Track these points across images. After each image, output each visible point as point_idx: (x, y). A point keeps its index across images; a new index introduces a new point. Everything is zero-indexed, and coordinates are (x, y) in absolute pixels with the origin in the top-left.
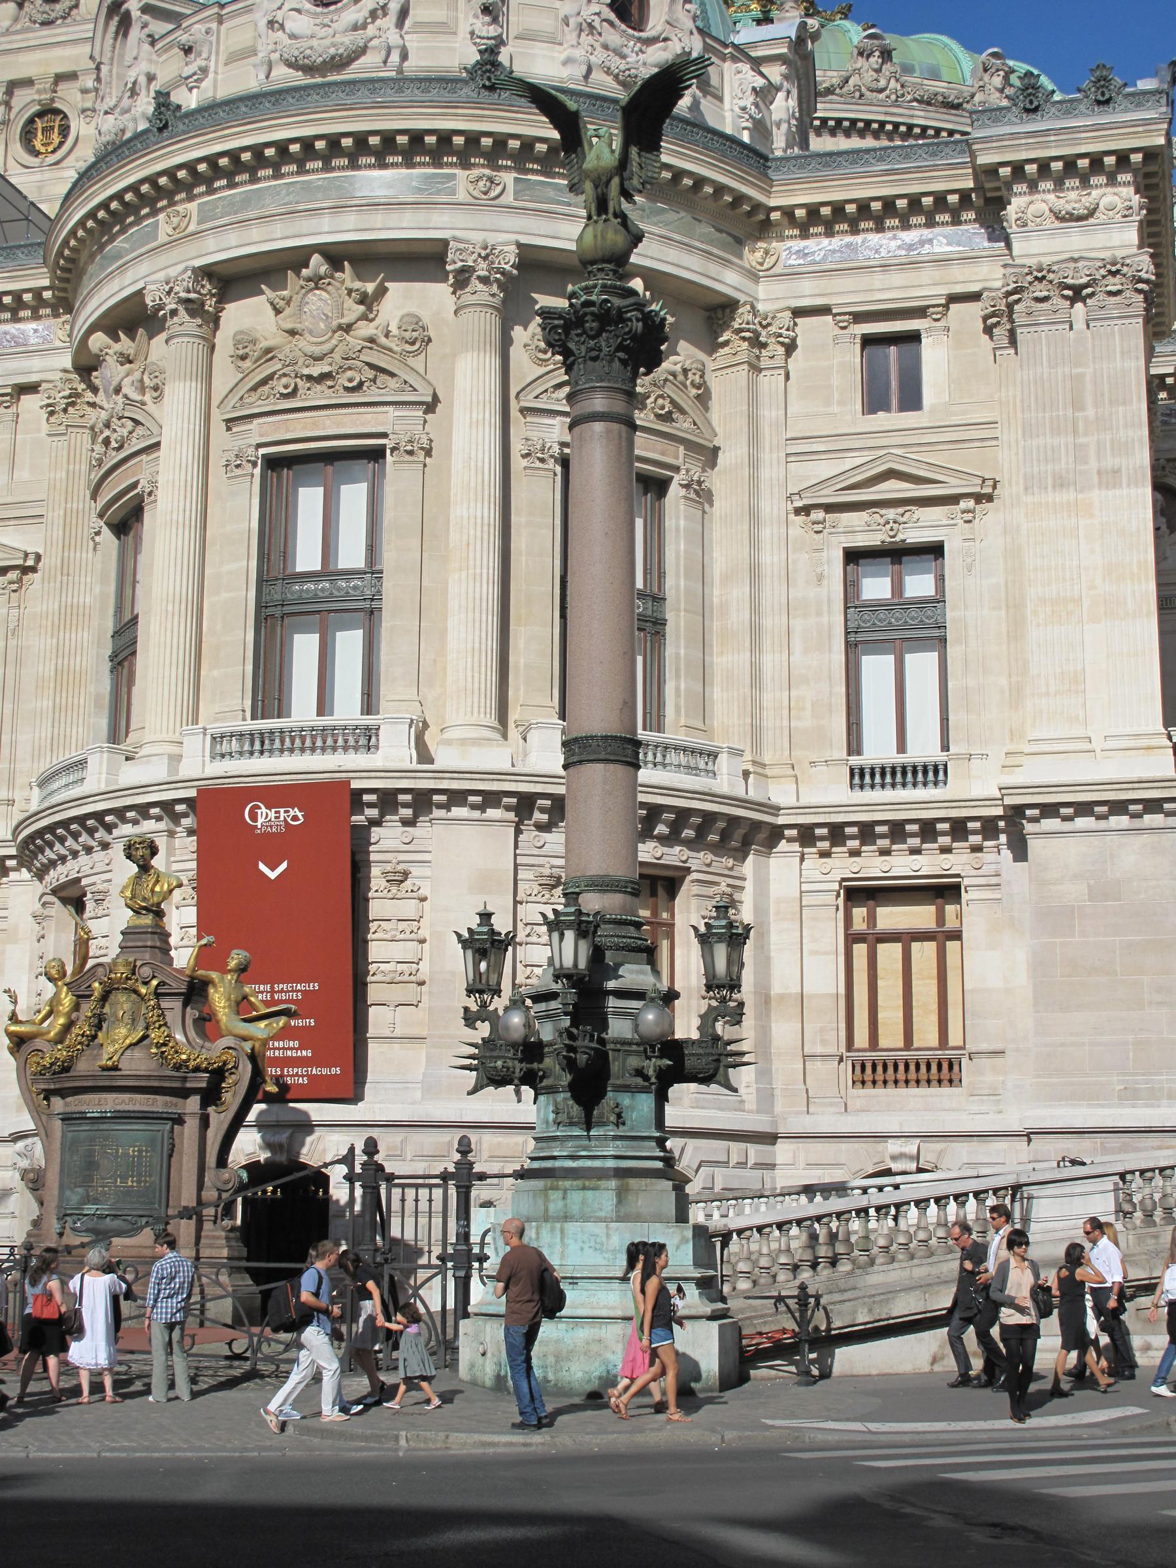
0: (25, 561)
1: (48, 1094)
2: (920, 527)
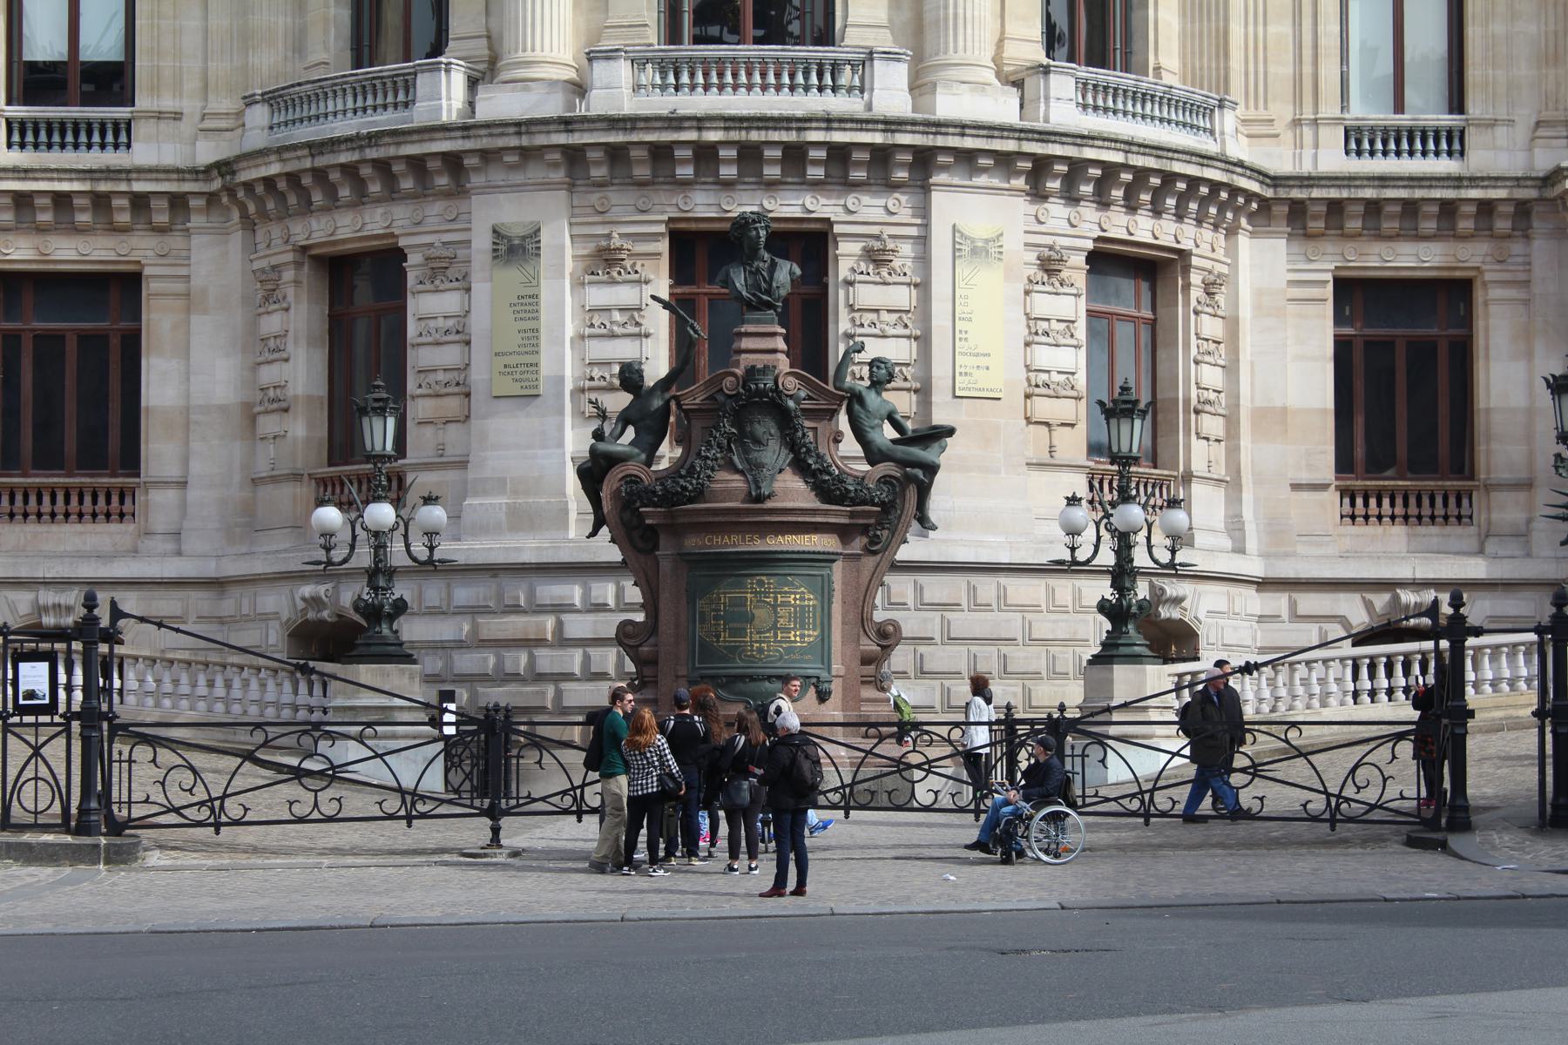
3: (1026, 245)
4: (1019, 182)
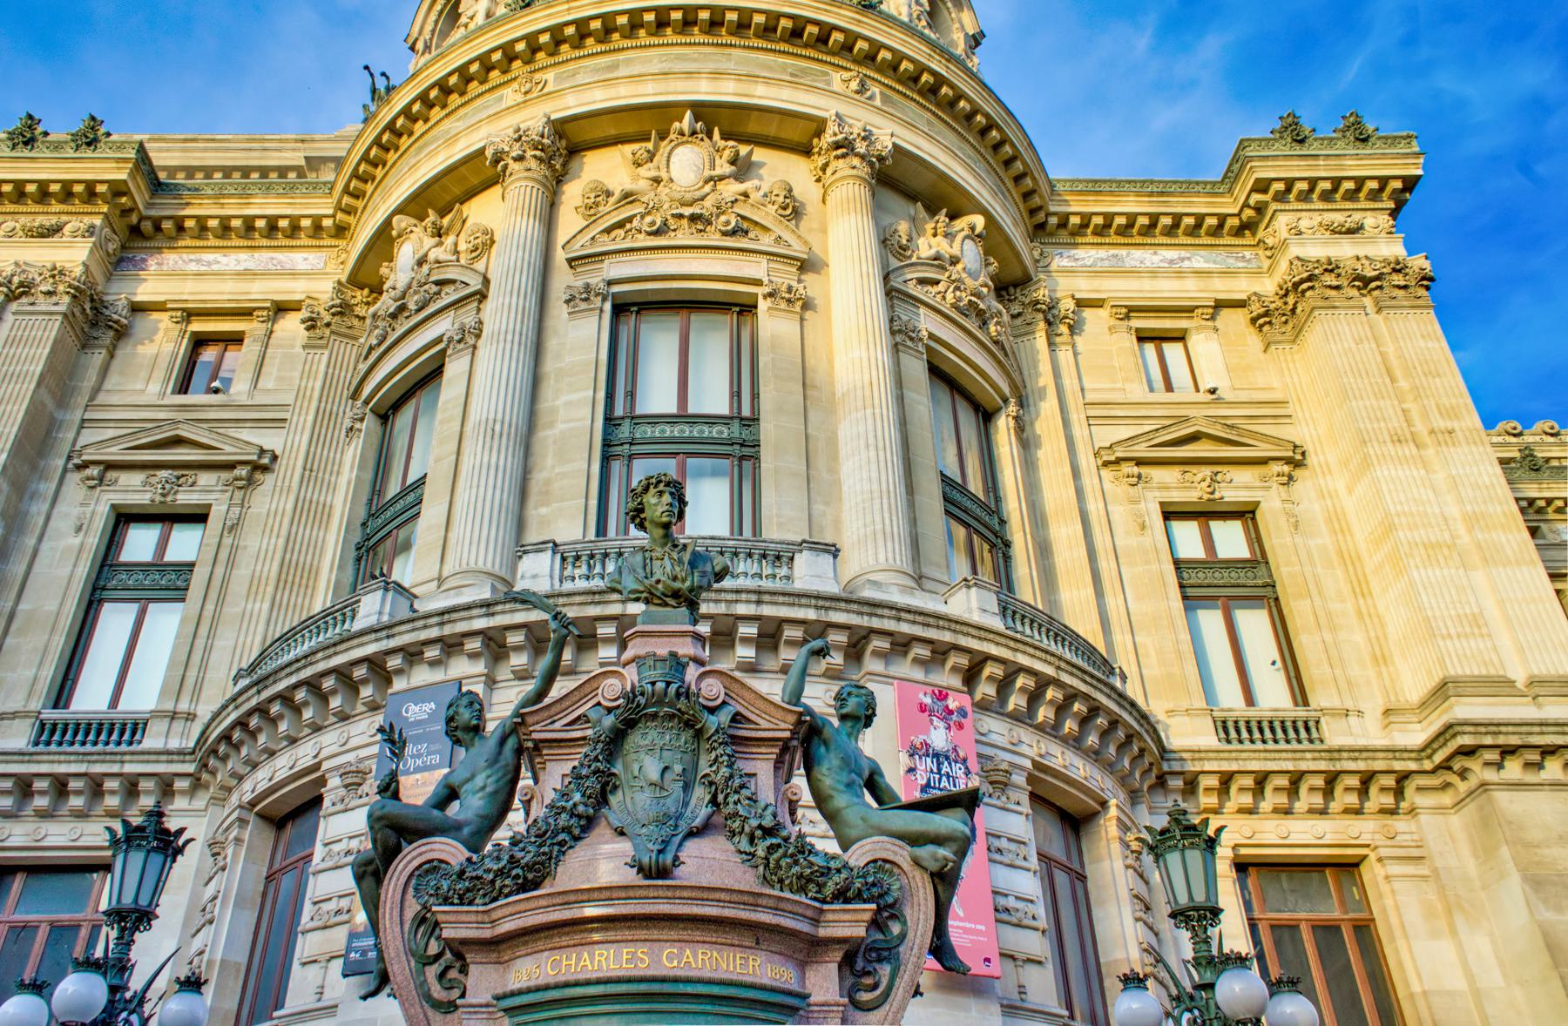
0: (260, 457)
2: (1238, 486)
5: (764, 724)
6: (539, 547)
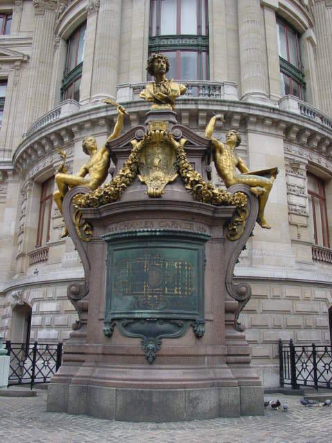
1: (91, 224)
3: (285, 158)
4: (281, 133)
5: (197, 145)
6: (125, 86)
